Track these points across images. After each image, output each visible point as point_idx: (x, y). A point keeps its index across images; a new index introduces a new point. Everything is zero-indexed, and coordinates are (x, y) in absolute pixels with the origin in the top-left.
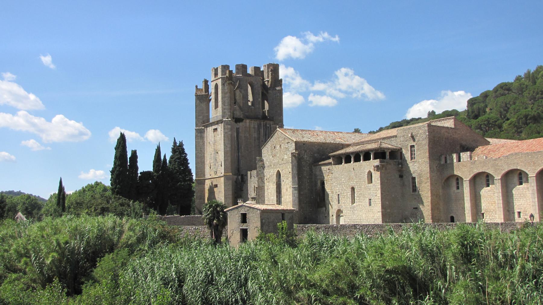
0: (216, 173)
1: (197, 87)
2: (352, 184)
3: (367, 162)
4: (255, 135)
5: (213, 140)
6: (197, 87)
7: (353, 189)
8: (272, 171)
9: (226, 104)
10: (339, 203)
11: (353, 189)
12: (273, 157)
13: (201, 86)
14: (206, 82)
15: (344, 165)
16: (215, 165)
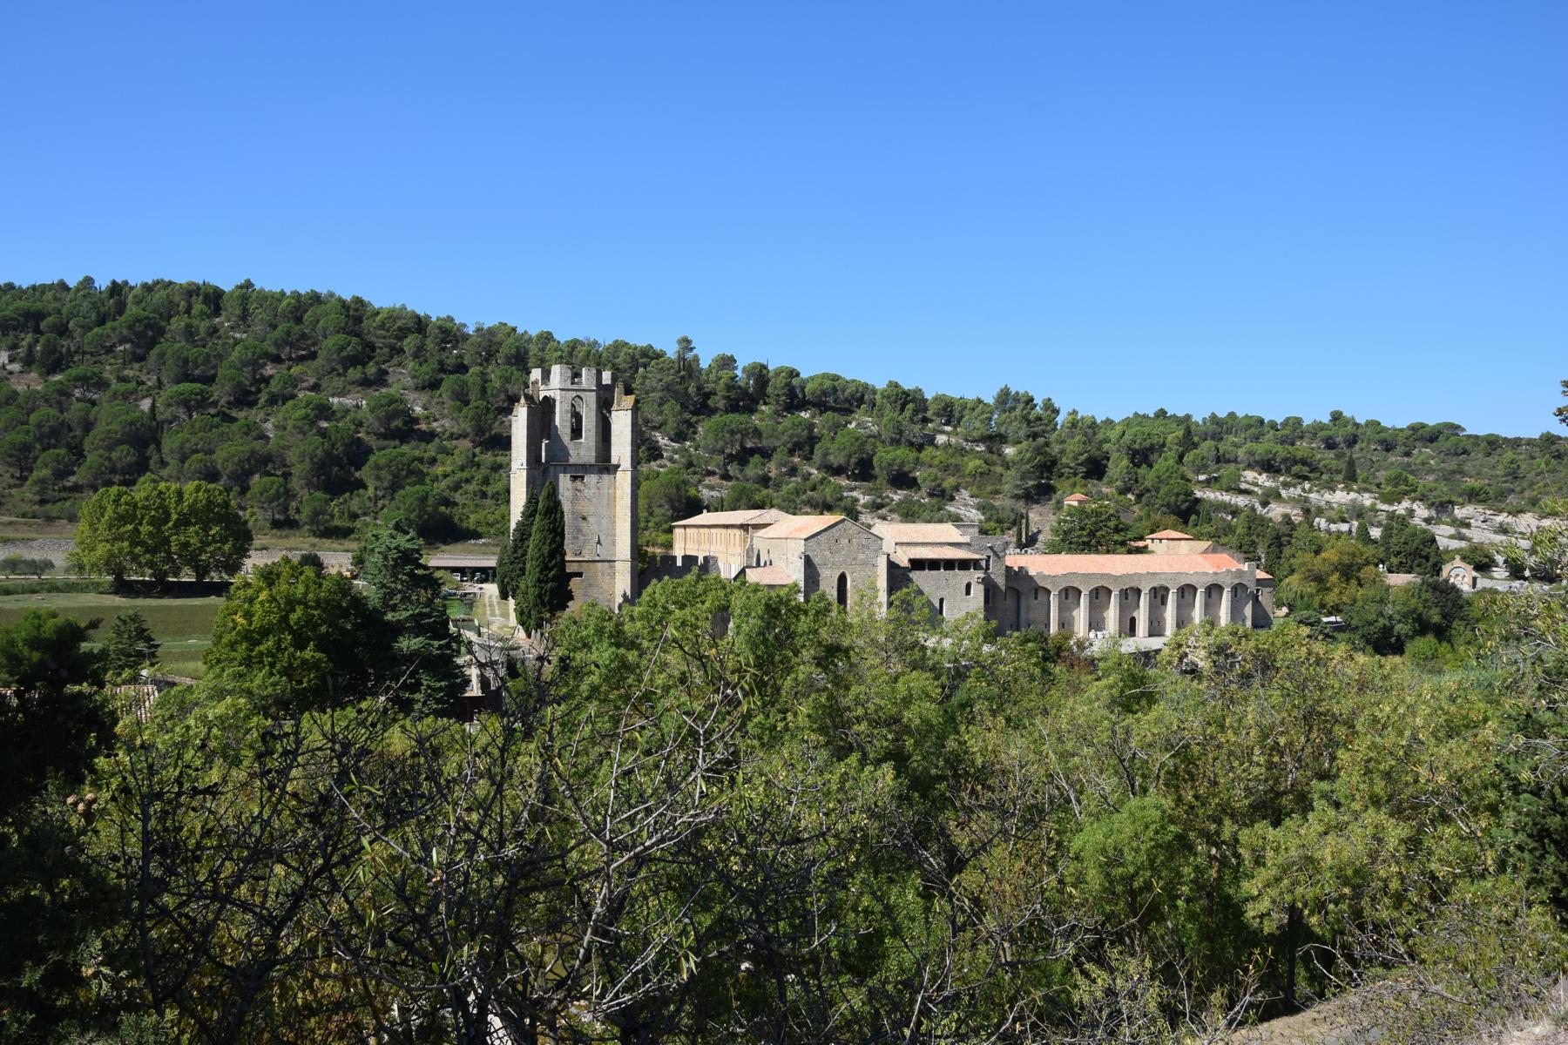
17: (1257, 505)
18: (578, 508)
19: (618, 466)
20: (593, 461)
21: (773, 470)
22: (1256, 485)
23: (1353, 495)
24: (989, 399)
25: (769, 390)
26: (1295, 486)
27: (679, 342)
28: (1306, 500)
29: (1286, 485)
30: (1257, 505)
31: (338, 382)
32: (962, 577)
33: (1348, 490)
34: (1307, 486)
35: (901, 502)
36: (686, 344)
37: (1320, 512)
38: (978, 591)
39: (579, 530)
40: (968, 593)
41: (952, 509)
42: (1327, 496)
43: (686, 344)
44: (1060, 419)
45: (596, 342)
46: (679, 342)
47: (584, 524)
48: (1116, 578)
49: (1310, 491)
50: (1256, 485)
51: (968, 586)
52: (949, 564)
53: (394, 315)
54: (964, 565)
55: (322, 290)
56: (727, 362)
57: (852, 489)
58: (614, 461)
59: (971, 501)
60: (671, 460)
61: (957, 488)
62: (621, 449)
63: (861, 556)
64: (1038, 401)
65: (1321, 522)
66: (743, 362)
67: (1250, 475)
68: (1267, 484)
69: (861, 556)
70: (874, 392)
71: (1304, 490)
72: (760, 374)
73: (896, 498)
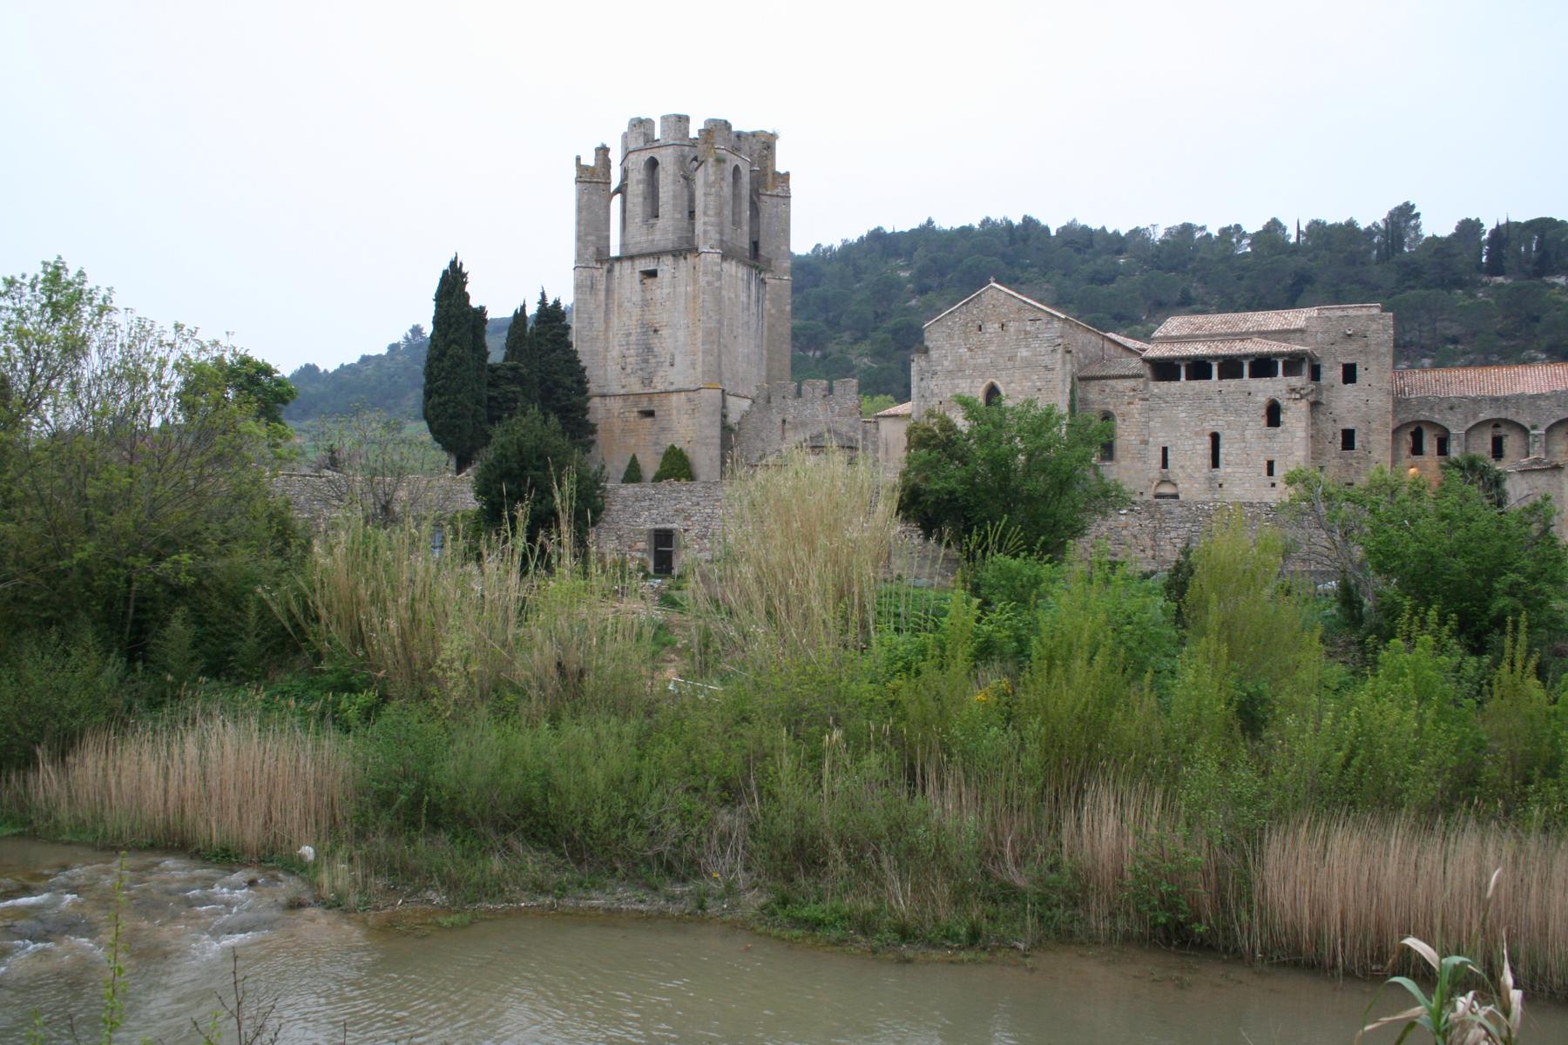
0: (648, 381)
1: (578, 159)
2: (1210, 427)
3: (1232, 383)
4: (743, 298)
5: (637, 298)
6: (578, 159)
7: (1215, 438)
9: (711, 212)
10: (1215, 463)
11: (1215, 438)
12: (970, 350)
13: (589, 160)
14: (603, 151)
15: (1184, 385)
16: (646, 361)
18: (648, 317)
39: (649, 349)
52: (1231, 368)
54: (1263, 366)
63: (1024, 352)
66: (1489, 226)
69: (1024, 352)
72: (1506, 234)
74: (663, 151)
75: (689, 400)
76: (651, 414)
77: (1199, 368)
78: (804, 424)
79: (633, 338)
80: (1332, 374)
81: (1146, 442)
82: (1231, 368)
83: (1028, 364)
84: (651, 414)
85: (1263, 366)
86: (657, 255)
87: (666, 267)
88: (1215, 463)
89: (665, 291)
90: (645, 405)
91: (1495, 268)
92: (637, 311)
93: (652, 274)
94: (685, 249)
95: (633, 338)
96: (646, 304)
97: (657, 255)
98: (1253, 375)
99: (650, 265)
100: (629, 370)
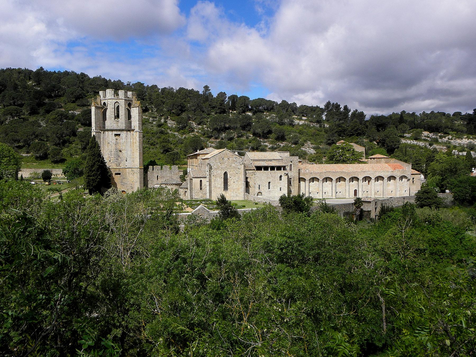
2: (269, 180)
8: (219, 172)
11: (269, 183)
16: (118, 159)
17: (428, 145)
19: (134, 130)
20: (124, 128)
21: (235, 135)
22: (428, 137)
23: (470, 140)
24: (322, 106)
25: (237, 105)
26: (445, 137)
27: (204, 87)
28: (449, 143)
29: (441, 137)
30: (428, 145)
31: (73, 105)
32: (279, 173)
33: (468, 138)
34: (450, 137)
35: (284, 146)
36: (206, 88)
37: (455, 147)
38: (285, 178)
39: (119, 156)
40: (281, 179)
41: (304, 149)
42: (459, 141)
43: (206, 88)
44: (350, 113)
45: (172, 88)
46: (204, 87)
47: (120, 154)
48: (348, 174)
49: (451, 139)
50: (428, 137)
51: (281, 177)
52: (273, 168)
53: (96, 79)
54: (279, 168)
55: (70, 70)
56: (222, 95)
57: (265, 142)
58: (133, 128)
59: (311, 146)
60: (197, 132)
61: (305, 141)
62: (135, 123)
64: (342, 106)
65: (455, 151)
66: (228, 95)
67: (426, 133)
68: (433, 137)
69: (233, 165)
70: (277, 104)
71: (449, 139)
72: (233, 98)
73: (282, 145)
74: (121, 100)
75: (132, 170)
76: (120, 174)
77: (266, 168)
78: (163, 177)
79: (113, 153)
80: (288, 168)
81: (255, 184)
82: (273, 168)
83: (234, 167)
84: (120, 174)
85: (279, 168)
86: (122, 130)
87: (123, 134)
88: (269, 188)
89: (124, 140)
90: (118, 172)
91: (233, 108)
92: (114, 146)
93: (119, 135)
94: (129, 129)
95: (113, 153)
96: (116, 144)
97: (122, 130)
98: (277, 170)
99: (119, 133)
100: (111, 161)
